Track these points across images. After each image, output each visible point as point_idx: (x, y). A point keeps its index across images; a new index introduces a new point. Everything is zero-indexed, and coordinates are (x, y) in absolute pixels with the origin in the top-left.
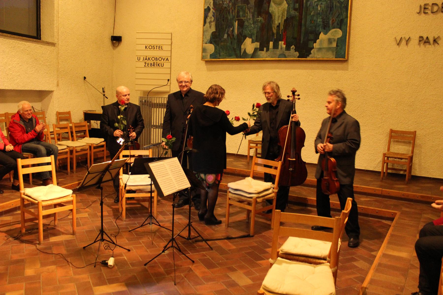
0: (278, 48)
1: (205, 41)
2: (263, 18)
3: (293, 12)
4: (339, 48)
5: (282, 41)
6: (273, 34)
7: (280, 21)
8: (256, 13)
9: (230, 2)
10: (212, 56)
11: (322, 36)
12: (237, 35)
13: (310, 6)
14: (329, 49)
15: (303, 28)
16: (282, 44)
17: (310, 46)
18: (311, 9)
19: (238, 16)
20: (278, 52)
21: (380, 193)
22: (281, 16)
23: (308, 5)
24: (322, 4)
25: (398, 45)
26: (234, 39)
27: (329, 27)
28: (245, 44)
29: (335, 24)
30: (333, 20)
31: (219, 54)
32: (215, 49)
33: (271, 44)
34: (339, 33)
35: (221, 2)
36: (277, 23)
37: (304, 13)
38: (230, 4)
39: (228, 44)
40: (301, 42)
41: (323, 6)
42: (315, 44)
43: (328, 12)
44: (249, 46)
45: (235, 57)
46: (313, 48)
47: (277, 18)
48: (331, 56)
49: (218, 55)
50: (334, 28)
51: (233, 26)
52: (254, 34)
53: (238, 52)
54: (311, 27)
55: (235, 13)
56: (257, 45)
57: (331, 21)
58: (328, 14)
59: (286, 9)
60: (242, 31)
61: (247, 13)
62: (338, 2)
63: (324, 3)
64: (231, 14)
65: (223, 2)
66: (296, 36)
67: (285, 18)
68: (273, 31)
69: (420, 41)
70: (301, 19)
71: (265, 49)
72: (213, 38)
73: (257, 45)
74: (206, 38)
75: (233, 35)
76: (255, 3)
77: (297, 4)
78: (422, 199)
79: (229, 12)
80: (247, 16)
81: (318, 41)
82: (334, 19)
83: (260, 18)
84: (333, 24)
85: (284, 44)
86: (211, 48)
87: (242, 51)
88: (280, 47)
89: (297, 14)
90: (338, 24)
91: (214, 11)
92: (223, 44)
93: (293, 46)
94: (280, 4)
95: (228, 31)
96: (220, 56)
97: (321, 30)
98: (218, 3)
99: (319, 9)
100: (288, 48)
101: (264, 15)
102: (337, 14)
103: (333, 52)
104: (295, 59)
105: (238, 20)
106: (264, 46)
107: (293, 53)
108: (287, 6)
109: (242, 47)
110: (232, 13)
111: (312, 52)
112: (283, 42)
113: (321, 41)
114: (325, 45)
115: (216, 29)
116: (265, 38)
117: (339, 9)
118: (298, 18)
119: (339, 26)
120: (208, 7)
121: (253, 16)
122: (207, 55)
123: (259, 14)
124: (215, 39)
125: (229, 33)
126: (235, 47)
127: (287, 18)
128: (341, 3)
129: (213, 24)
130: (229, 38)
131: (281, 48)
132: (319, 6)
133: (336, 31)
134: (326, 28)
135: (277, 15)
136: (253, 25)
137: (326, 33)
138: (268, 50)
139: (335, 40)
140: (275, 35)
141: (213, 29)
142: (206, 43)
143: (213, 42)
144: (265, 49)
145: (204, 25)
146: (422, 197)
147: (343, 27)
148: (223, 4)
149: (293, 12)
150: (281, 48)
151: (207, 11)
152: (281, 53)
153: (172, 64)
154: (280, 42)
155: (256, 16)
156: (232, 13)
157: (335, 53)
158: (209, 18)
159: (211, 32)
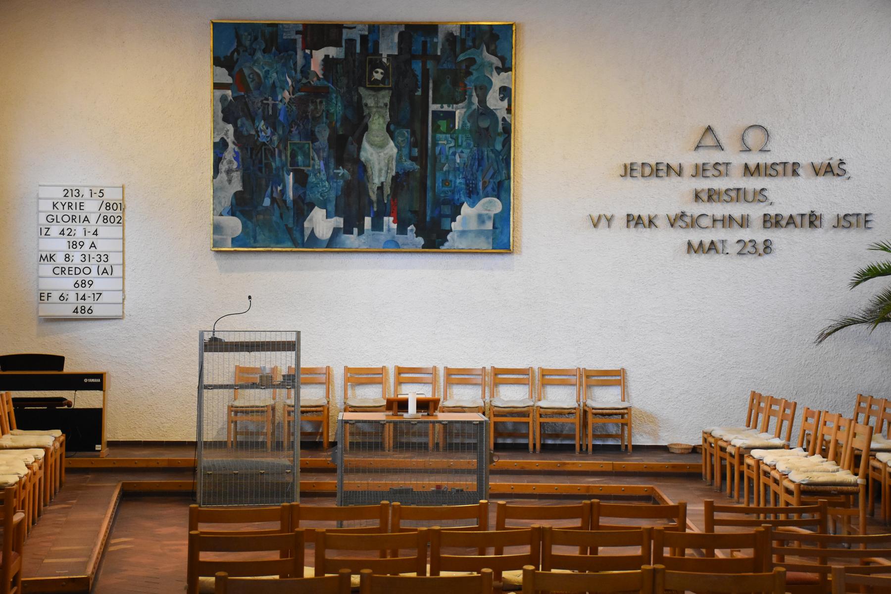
0: (381, 229)
1: (220, 209)
2: (348, 171)
3: (408, 164)
4: (498, 231)
5: (389, 216)
6: (371, 203)
7: (383, 179)
8: (332, 161)
9: (273, 134)
10: (236, 241)
11: (465, 209)
12: (294, 201)
13: (440, 153)
14: (480, 233)
15: (429, 195)
16: (389, 222)
17: (445, 226)
18: (443, 161)
19: (294, 163)
20: (383, 236)
21: (610, 469)
22: (385, 169)
23: (437, 151)
24: (462, 152)
25: (595, 226)
26: (288, 208)
27: (478, 193)
28: (311, 220)
29: (489, 189)
30: (484, 183)
31: (255, 238)
32: (244, 226)
33: (368, 221)
34: (497, 206)
35: (253, 132)
36: (377, 181)
37: (429, 166)
38: (275, 138)
39: (275, 218)
40: (428, 219)
41: (465, 155)
42: (453, 224)
43: (475, 167)
44: (321, 223)
45: (290, 244)
46: (451, 230)
47: (376, 173)
48: (484, 244)
49: (252, 241)
50: (487, 196)
51: (282, 181)
52: (330, 201)
53: (297, 235)
54: (444, 192)
55: (287, 157)
56: (339, 222)
57: (480, 184)
58: (474, 171)
59: (395, 156)
60: (305, 193)
61: (313, 159)
62: (492, 150)
63: (467, 151)
64: (277, 158)
65: (257, 132)
66: (416, 207)
67: (394, 173)
68: (369, 197)
69: (628, 221)
70: (424, 178)
71: (355, 230)
72: (237, 204)
73: (339, 222)
74: (220, 203)
75: (285, 201)
76: (329, 139)
77: (416, 150)
78: (675, 471)
79: (273, 155)
80: (314, 165)
81: (458, 218)
82: (487, 179)
83: (341, 171)
84: (484, 188)
85: (394, 222)
86: (235, 225)
87: (307, 233)
88: (385, 227)
89: (417, 167)
90: (494, 190)
91: (237, 149)
92: (261, 217)
93: (412, 227)
94: (382, 146)
95: (272, 192)
96: (255, 242)
97: (463, 199)
98: (245, 133)
99: (458, 161)
100: (402, 230)
101: (349, 166)
102: (491, 172)
103: (488, 238)
104: (418, 250)
105: (293, 171)
106: (352, 224)
107: (412, 237)
108: (395, 150)
109: (306, 224)
110: (280, 156)
111: (449, 237)
112: (391, 219)
113: (464, 218)
114: (473, 225)
115: (244, 186)
116: (356, 208)
117: (495, 164)
118: (418, 175)
119: (495, 193)
120: (222, 138)
121: (327, 165)
122: (225, 240)
123: (340, 162)
124: (242, 205)
125: (275, 195)
126: (290, 226)
127: (397, 173)
128: (499, 153)
129: (237, 176)
130: (276, 206)
131: (389, 230)
132: (457, 156)
133: (490, 202)
134: (473, 194)
135: (376, 168)
136: (327, 184)
137: (472, 205)
138: (361, 232)
139: (489, 218)
140: (375, 205)
141: (237, 186)
142: (221, 215)
143: (238, 213)
144: (355, 230)
145: (215, 177)
146: (674, 466)
147: (503, 195)
148: (259, 136)
149: (408, 164)
150: (389, 230)
151: (220, 147)
152: (389, 238)
153: (126, 257)
154: (386, 219)
155: (332, 166)
156: (280, 156)
157: (491, 240)
158: (225, 162)
159: (233, 191)
